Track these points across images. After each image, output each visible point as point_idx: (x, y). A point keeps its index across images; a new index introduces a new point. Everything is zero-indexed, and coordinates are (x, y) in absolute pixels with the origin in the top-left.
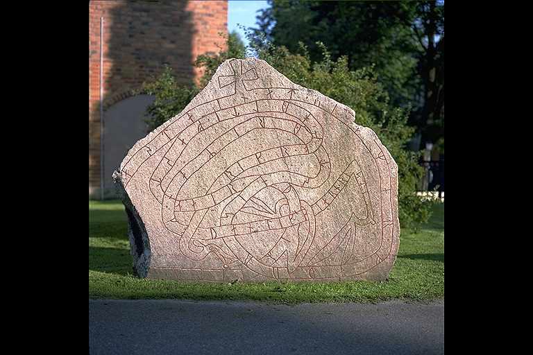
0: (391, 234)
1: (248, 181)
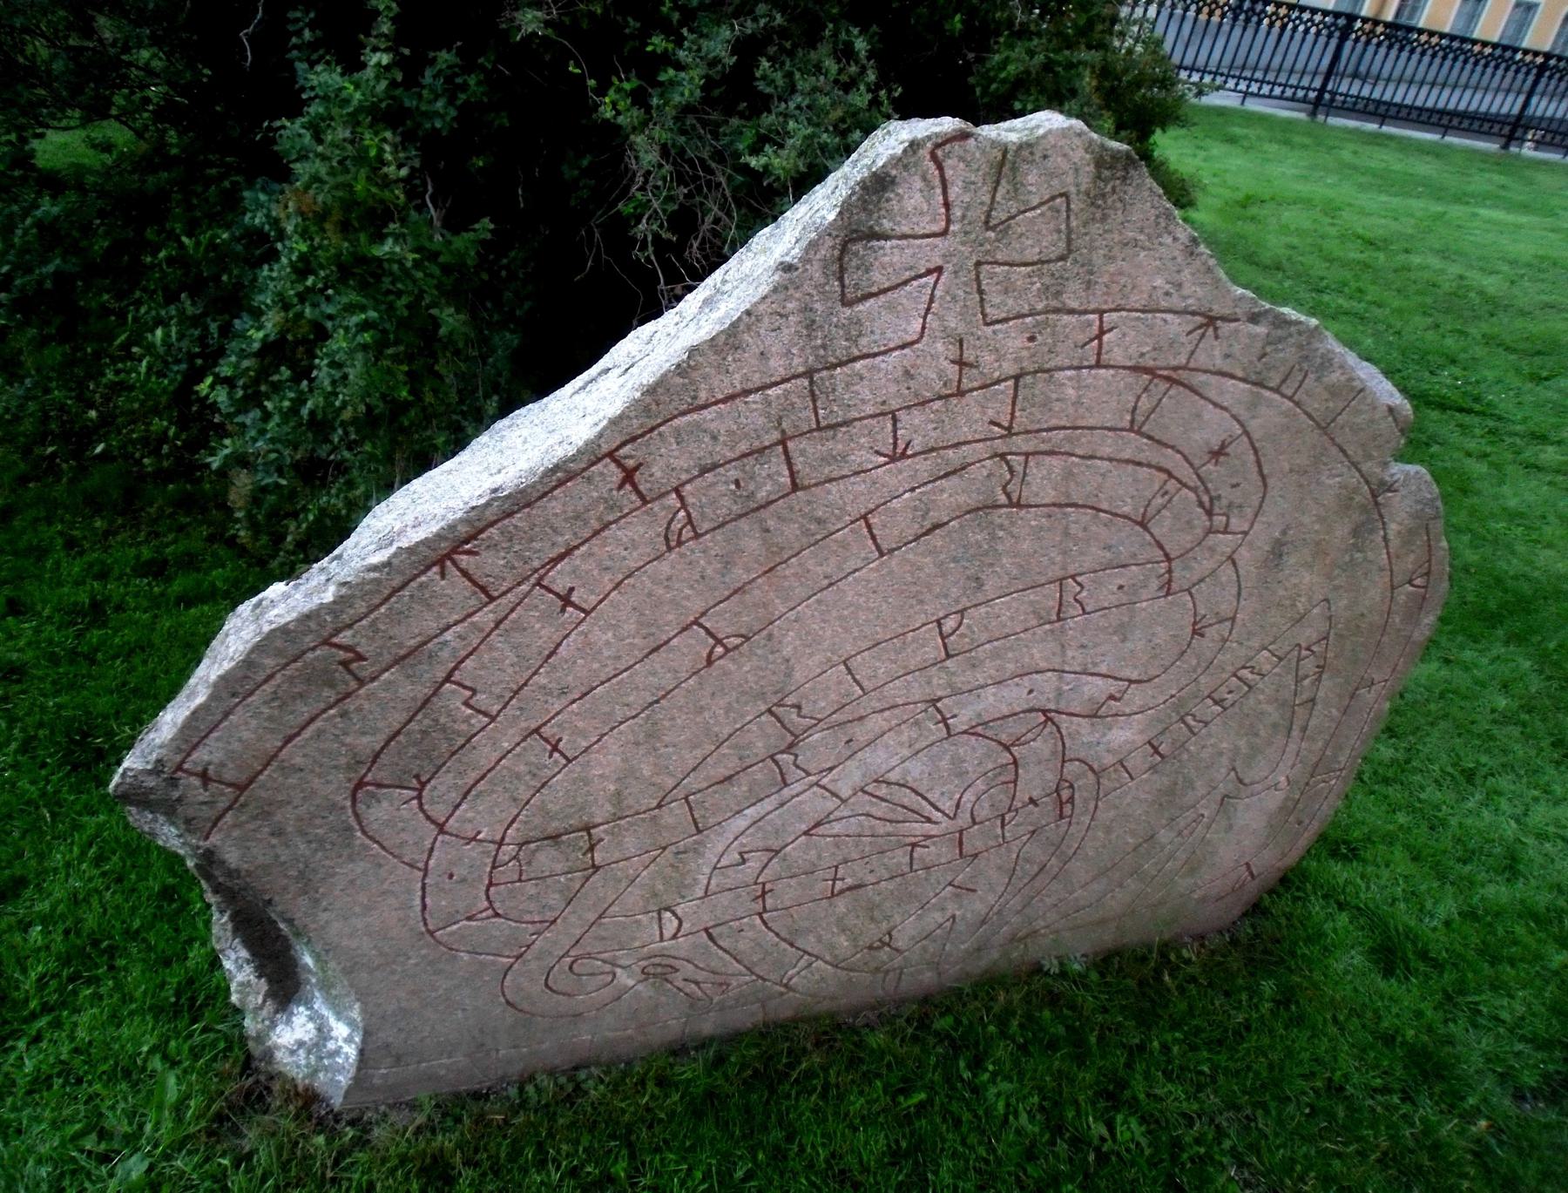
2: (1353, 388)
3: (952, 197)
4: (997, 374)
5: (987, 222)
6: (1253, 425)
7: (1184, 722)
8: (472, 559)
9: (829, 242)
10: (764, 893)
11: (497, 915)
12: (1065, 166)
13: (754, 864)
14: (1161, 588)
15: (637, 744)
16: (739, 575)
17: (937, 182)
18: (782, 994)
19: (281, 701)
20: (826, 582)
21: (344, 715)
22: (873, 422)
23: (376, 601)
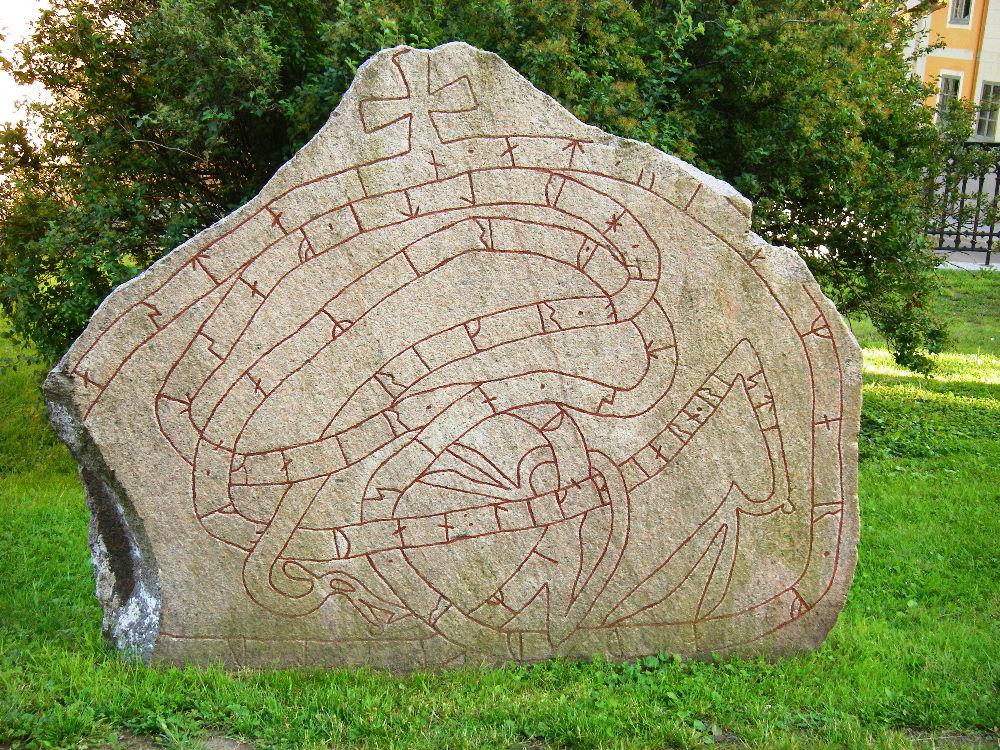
4: (456, 171)
6: (629, 206)
10: (400, 529)
11: (236, 511)
13: (390, 498)
16: (341, 282)
17: (398, 71)
18: (433, 636)
21: (151, 348)
22: (395, 195)
23: (165, 280)
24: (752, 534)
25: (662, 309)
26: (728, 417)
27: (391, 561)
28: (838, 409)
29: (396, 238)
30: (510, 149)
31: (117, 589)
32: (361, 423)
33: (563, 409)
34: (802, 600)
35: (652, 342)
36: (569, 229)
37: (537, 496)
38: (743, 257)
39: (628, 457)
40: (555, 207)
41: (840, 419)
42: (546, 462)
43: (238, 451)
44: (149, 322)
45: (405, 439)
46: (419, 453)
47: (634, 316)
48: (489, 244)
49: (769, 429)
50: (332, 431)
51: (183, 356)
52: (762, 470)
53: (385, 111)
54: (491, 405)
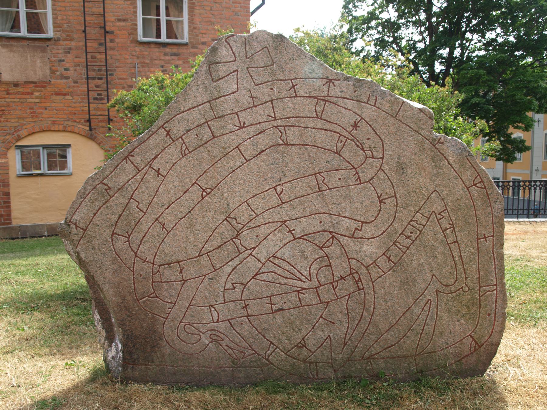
0: (494, 306)
1: (264, 230)
2: (399, 102)
3: (234, 51)
4: (264, 100)
5: (246, 57)
6: (364, 116)
7: (396, 245)
8: (133, 158)
9: (205, 65)
10: (246, 306)
11: (157, 297)
12: (263, 40)
13: (239, 289)
14: (356, 180)
15: (187, 228)
17: (229, 47)
18: (268, 365)
19: (92, 201)
20: (231, 170)
21: (107, 207)
22: (231, 116)
23: (112, 170)
24: (446, 304)
25: (386, 175)
26: (428, 237)
27: (242, 324)
28: (491, 230)
29: (232, 140)
30: (293, 86)
31: (107, 338)
32: (220, 246)
33: (333, 235)
34: (476, 343)
35: (381, 194)
36: (330, 131)
37: (321, 286)
38: (431, 143)
39: (372, 262)
40: (321, 118)
41: (493, 236)
42: (325, 266)
43: (155, 263)
44: (105, 193)
45: (244, 255)
46: (253, 262)
47: (371, 180)
48: (285, 141)
49: (452, 243)
50: (204, 251)
51: (123, 211)
52: (449, 267)
53: (223, 69)
54: (292, 234)
